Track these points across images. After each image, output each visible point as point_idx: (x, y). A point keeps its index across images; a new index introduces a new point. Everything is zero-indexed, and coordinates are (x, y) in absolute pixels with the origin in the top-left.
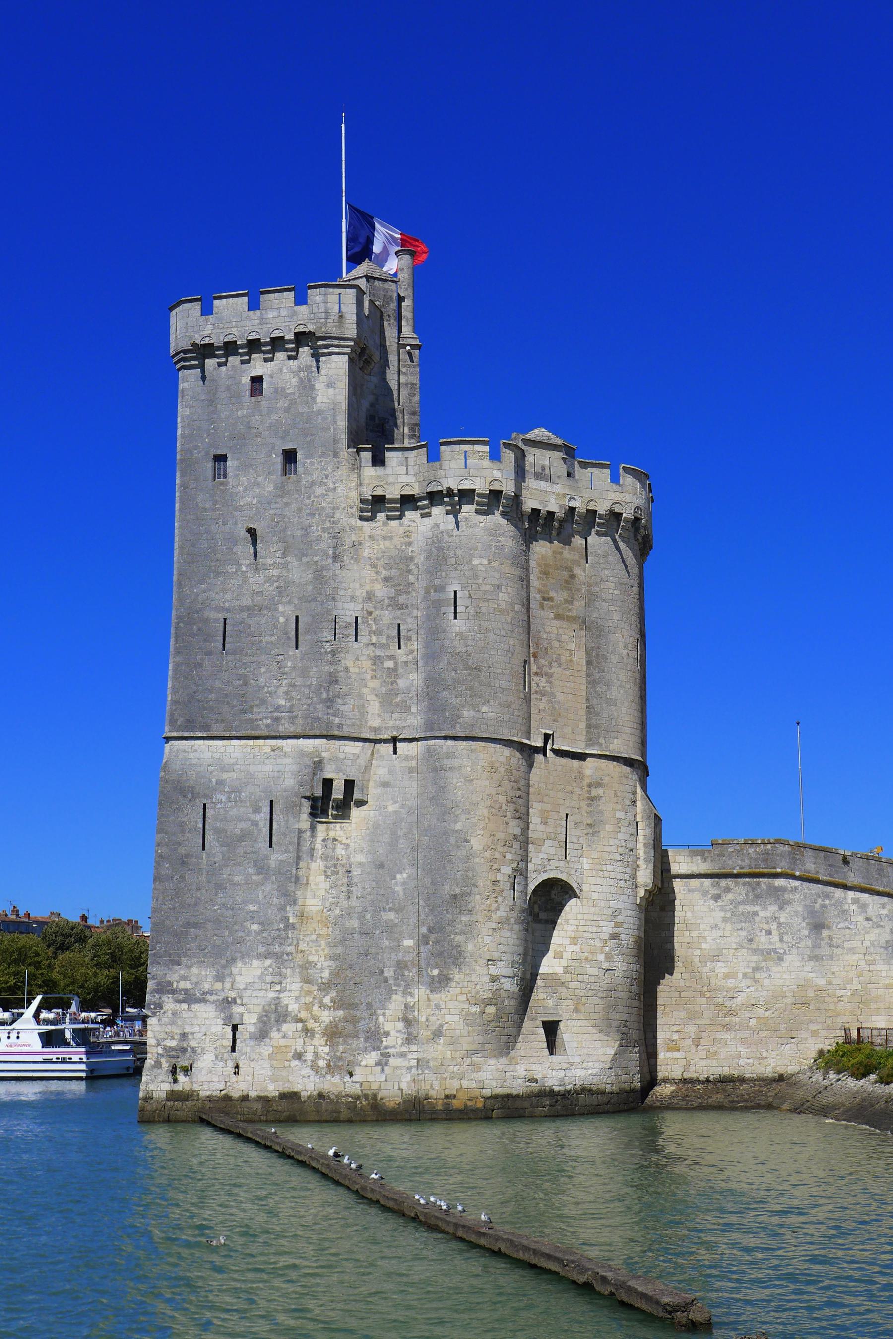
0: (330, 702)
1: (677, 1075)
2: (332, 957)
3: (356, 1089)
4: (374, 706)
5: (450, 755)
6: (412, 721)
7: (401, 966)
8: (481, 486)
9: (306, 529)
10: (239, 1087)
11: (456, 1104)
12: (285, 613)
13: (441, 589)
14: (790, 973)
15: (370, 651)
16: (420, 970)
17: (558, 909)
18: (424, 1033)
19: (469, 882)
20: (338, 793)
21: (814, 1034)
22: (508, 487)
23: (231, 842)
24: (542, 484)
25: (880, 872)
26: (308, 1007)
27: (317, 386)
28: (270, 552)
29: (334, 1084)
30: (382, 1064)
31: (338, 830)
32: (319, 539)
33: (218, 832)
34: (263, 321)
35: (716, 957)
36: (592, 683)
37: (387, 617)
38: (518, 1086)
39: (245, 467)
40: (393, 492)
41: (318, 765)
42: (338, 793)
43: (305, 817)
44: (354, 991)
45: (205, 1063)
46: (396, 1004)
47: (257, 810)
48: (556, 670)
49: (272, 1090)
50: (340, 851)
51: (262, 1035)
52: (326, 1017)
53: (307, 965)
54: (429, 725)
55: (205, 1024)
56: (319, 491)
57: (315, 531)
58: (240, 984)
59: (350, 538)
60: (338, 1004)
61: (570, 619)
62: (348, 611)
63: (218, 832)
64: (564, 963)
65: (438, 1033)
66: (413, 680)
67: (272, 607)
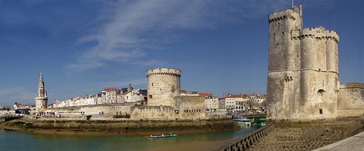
12: (282, 54)
16: (301, 103)
17: (322, 94)
42: (289, 78)
45: (273, 115)
49: (281, 119)
64: (323, 101)
67: (281, 53)
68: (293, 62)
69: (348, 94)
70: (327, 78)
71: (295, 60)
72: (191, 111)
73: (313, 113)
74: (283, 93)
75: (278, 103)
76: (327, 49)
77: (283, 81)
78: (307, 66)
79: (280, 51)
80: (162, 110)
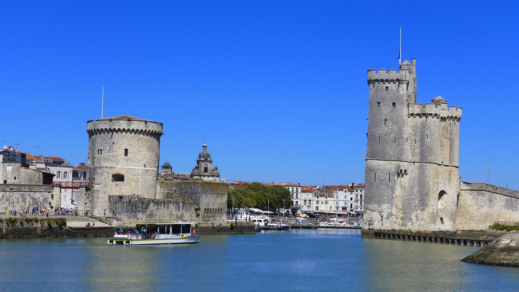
0: (401, 154)
1: (461, 229)
2: (402, 204)
3: (407, 229)
4: (410, 155)
5: (426, 166)
6: (418, 159)
7: (415, 206)
8: (433, 113)
9: (397, 119)
10: (383, 228)
11: (426, 233)
12: (392, 136)
13: (425, 133)
14: (485, 210)
15: (409, 144)
18: (420, 219)
19: (429, 191)
20: (403, 172)
21: (489, 222)
22: (438, 113)
23: (381, 181)
24: (443, 111)
25: (504, 191)
26: (397, 213)
27: (401, 90)
28: (389, 123)
29: (402, 228)
30: (412, 225)
31: (402, 179)
32: (400, 121)
33: (378, 178)
34: (389, 76)
35: (470, 206)
36: (450, 151)
37: (413, 137)
38: (437, 230)
39: (384, 105)
40: (415, 113)
41: (399, 167)
42: (403, 172)
43: (396, 177)
44: (406, 211)
45: (376, 223)
46: (414, 213)
47: (387, 175)
48: (444, 149)
49: (390, 229)
50: (403, 184)
51: (388, 218)
52: (401, 215)
53: (397, 205)
54: (421, 160)
55: (376, 216)
56: (400, 111)
57: (399, 120)
58: (383, 208)
59: (406, 121)
60: (403, 213)
61: (447, 138)
62: (405, 136)
63: (378, 178)
65: (423, 219)
66: (418, 150)
67: (390, 134)
68: (409, 151)
69: (471, 198)
70: (450, 175)
71: (411, 146)
72: (212, 211)
73: (434, 223)
74: (393, 192)
75: (385, 206)
76: (451, 134)
77: (394, 175)
78: (429, 158)
79: (389, 131)
80: (181, 208)
